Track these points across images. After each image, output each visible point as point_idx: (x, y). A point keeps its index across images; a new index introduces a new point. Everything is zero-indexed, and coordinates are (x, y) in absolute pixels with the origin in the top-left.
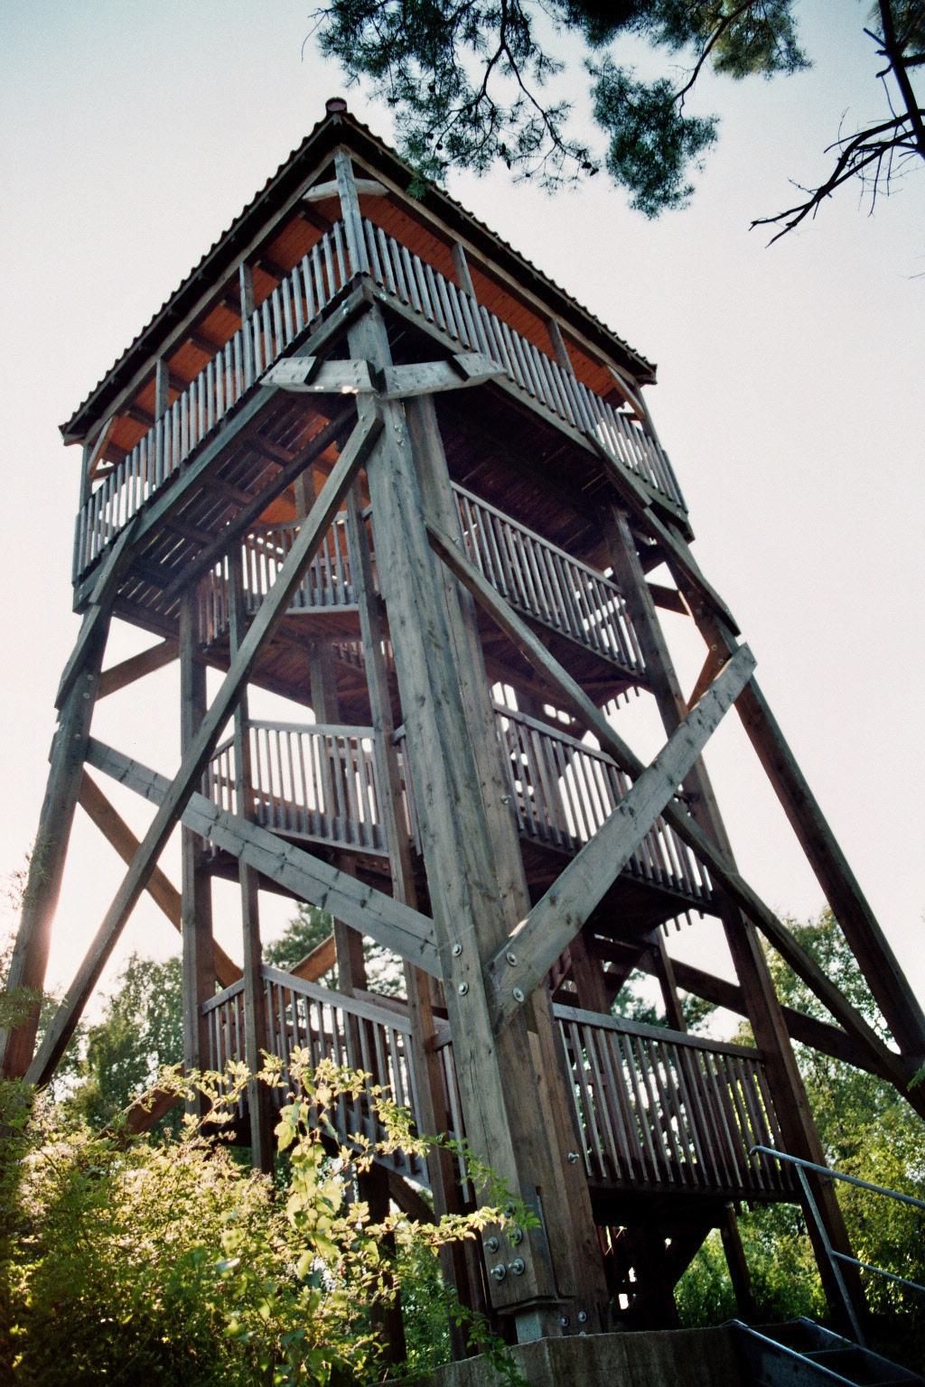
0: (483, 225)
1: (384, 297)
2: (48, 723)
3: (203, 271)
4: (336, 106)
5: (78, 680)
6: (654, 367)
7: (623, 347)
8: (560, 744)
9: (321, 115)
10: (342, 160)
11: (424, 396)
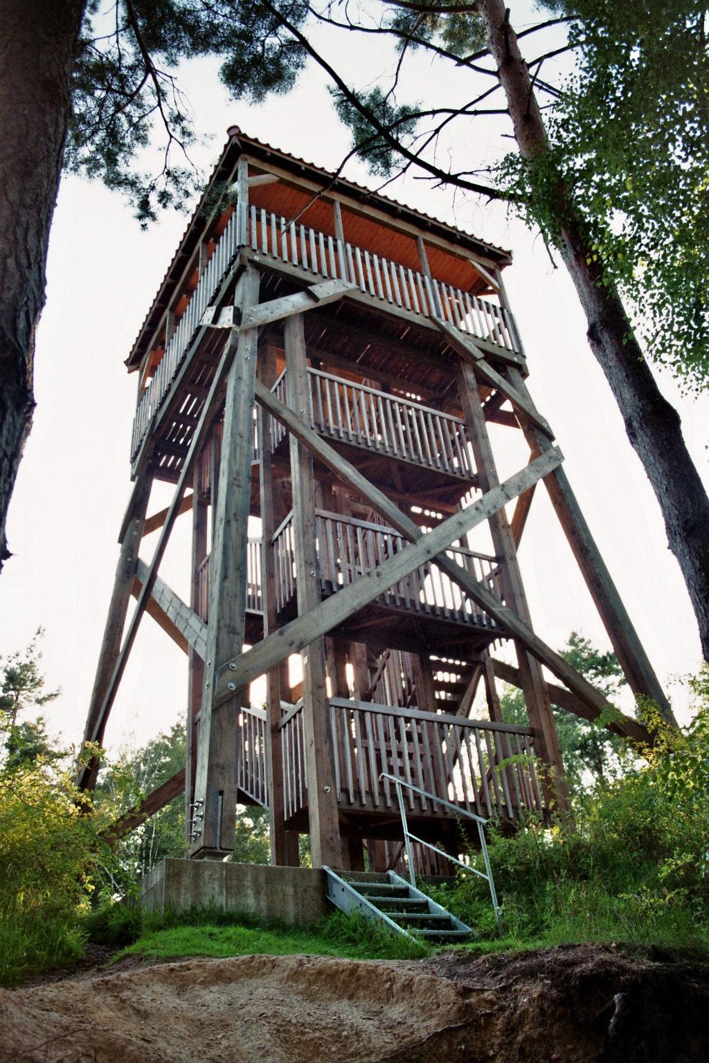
0: (355, 184)
1: (257, 258)
2: (114, 553)
3: (183, 251)
4: (234, 131)
5: (130, 524)
6: (509, 253)
7: (481, 244)
8: (390, 536)
9: (226, 139)
10: (242, 167)
11: (295, 316)
